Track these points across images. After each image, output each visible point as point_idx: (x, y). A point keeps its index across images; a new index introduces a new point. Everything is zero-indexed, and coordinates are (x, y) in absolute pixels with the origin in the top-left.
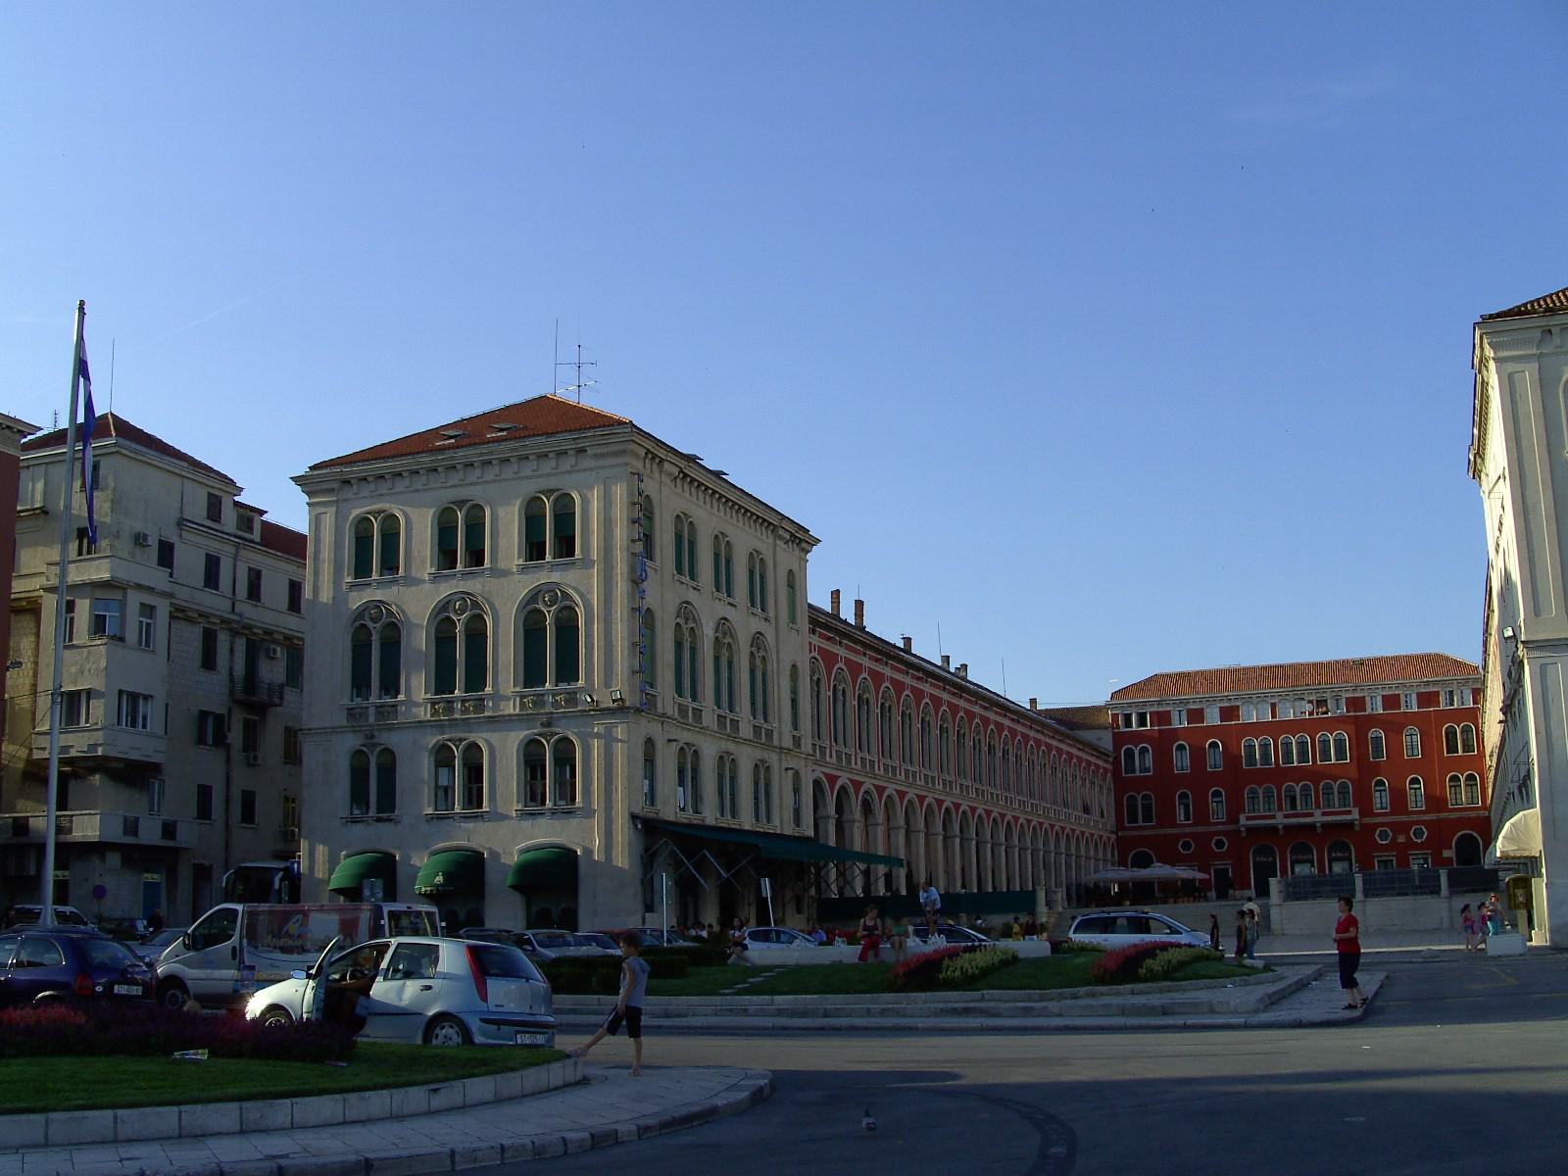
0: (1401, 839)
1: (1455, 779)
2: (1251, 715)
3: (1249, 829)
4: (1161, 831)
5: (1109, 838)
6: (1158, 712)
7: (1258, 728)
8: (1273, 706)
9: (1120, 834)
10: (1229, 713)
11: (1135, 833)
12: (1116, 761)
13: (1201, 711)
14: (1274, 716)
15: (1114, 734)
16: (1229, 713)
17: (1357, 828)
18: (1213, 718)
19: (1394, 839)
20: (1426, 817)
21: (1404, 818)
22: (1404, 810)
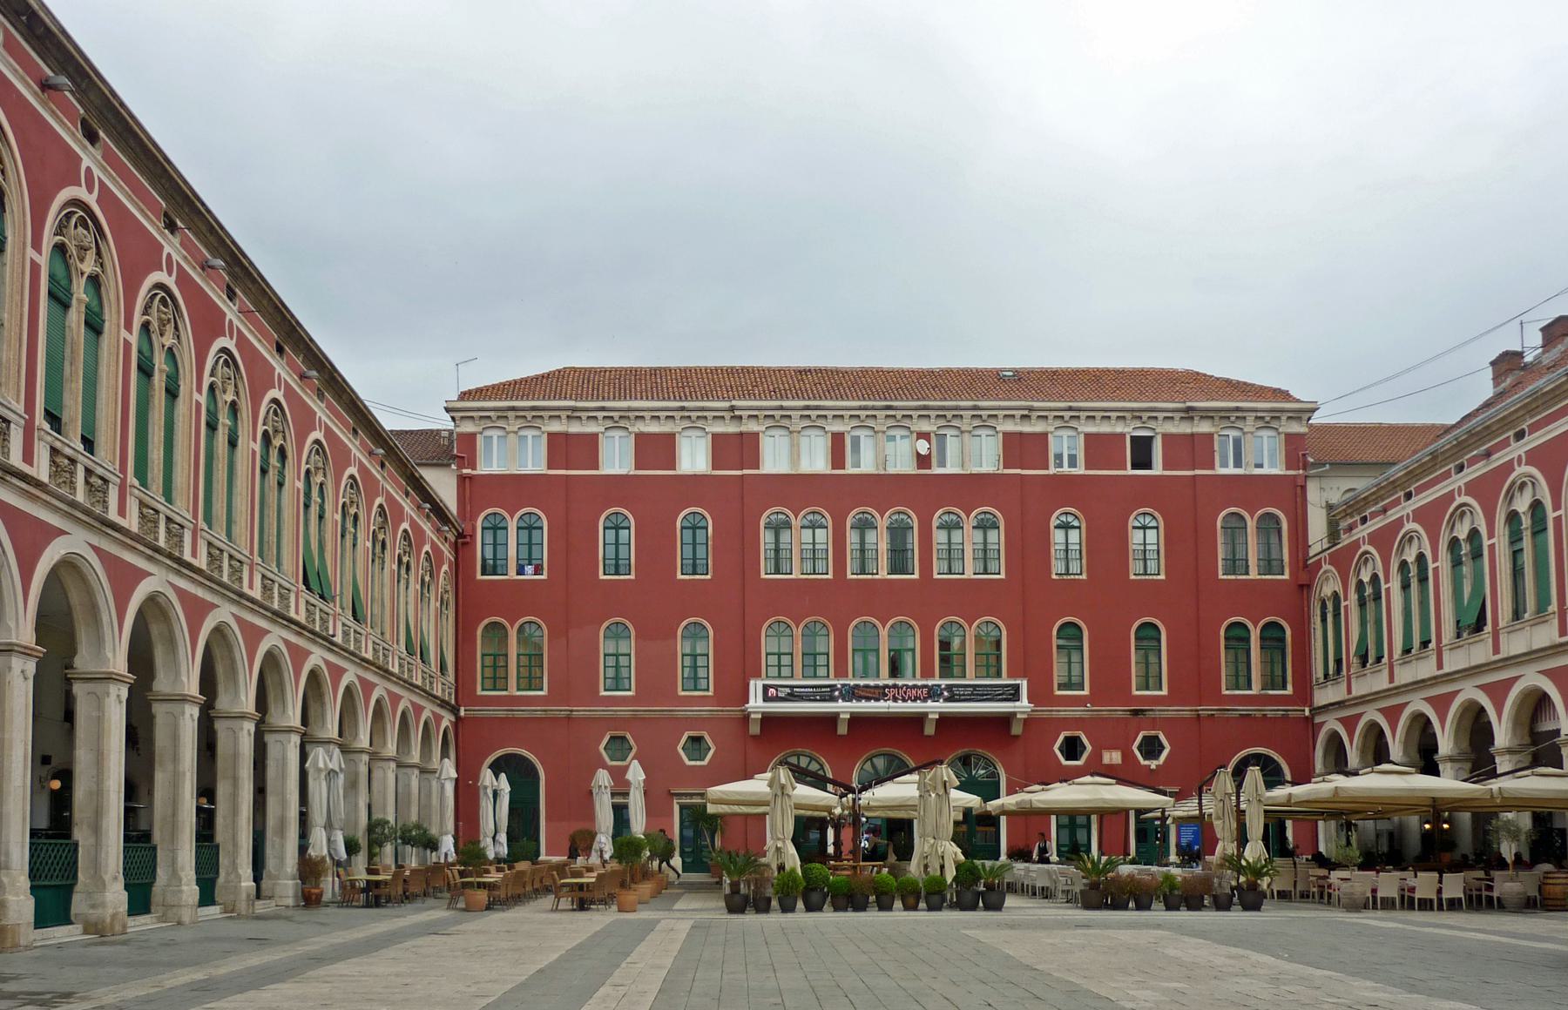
0: (1113, 757)
1: (1238, 637)
2: (775, 458)
3: (768, 720)
4: (560, 710)
5: (438, 718)
6: (566, 435)
7: (797, 489)
8: (838, 439)
9: (462, 713)
10: (737, 450)
11: (499, 712)
12: (462, 543)
13: (669, 440)
14: (838, 458)
15: (462, 480)
16: (737, 450)
17: (1017, 730)
18: (694, 458)
19: (1097, 755)
20: (1172, 711)
21: (1119, 711)
22: (1124, 695)
